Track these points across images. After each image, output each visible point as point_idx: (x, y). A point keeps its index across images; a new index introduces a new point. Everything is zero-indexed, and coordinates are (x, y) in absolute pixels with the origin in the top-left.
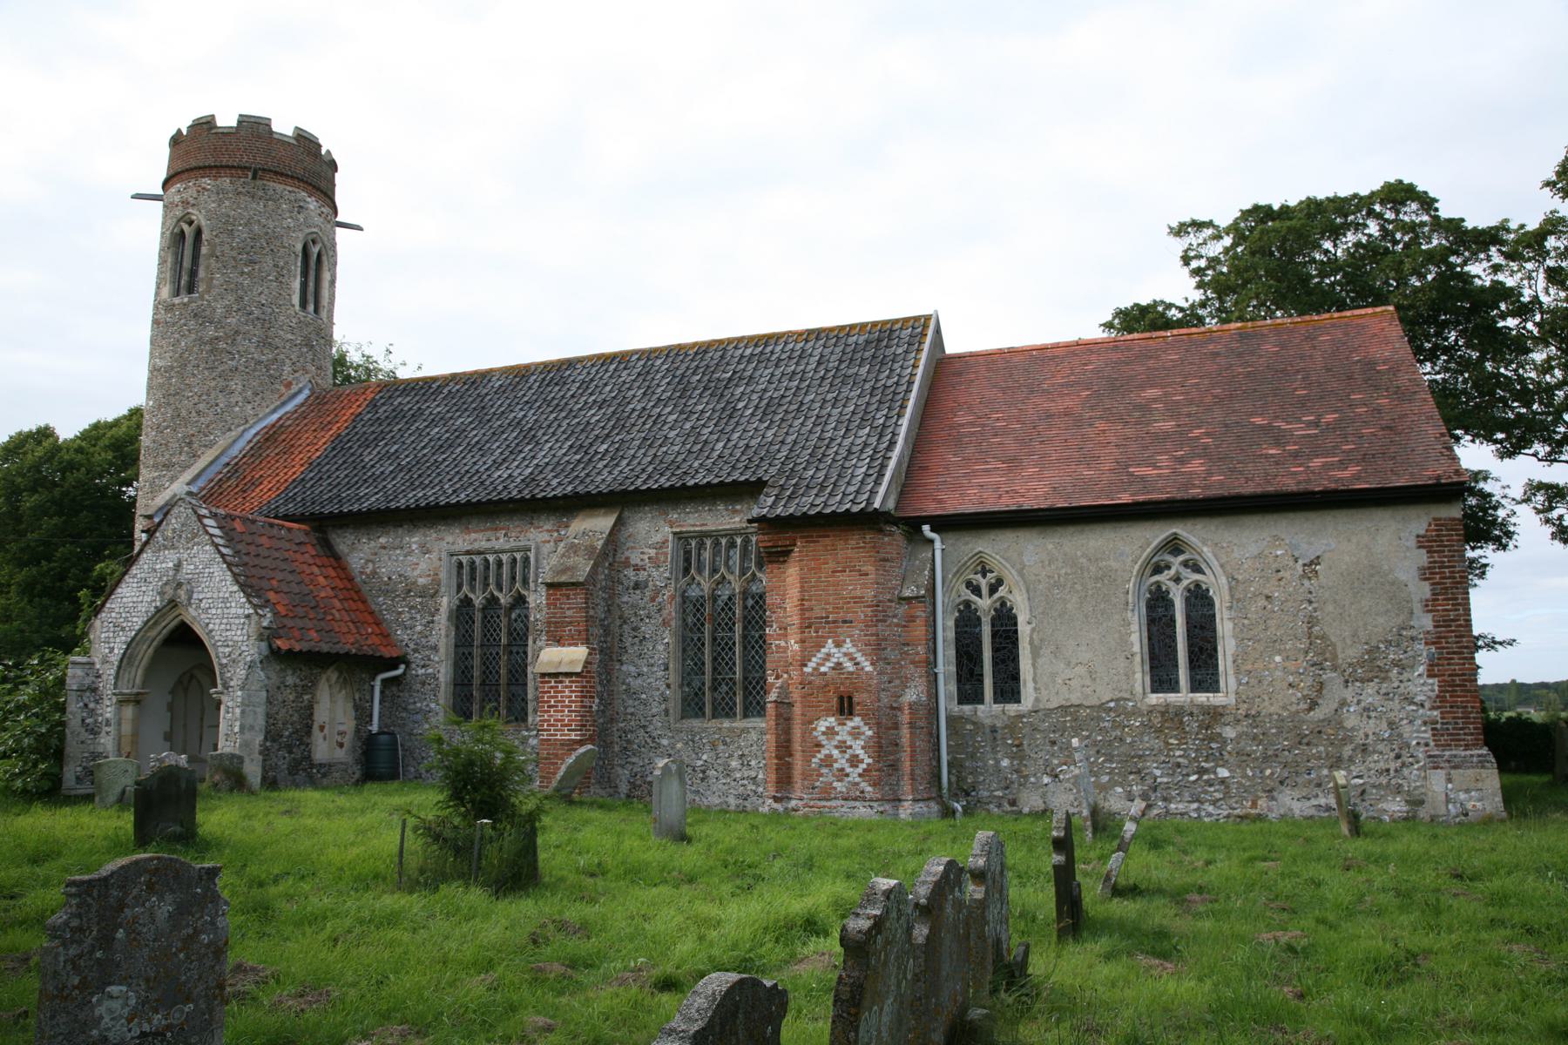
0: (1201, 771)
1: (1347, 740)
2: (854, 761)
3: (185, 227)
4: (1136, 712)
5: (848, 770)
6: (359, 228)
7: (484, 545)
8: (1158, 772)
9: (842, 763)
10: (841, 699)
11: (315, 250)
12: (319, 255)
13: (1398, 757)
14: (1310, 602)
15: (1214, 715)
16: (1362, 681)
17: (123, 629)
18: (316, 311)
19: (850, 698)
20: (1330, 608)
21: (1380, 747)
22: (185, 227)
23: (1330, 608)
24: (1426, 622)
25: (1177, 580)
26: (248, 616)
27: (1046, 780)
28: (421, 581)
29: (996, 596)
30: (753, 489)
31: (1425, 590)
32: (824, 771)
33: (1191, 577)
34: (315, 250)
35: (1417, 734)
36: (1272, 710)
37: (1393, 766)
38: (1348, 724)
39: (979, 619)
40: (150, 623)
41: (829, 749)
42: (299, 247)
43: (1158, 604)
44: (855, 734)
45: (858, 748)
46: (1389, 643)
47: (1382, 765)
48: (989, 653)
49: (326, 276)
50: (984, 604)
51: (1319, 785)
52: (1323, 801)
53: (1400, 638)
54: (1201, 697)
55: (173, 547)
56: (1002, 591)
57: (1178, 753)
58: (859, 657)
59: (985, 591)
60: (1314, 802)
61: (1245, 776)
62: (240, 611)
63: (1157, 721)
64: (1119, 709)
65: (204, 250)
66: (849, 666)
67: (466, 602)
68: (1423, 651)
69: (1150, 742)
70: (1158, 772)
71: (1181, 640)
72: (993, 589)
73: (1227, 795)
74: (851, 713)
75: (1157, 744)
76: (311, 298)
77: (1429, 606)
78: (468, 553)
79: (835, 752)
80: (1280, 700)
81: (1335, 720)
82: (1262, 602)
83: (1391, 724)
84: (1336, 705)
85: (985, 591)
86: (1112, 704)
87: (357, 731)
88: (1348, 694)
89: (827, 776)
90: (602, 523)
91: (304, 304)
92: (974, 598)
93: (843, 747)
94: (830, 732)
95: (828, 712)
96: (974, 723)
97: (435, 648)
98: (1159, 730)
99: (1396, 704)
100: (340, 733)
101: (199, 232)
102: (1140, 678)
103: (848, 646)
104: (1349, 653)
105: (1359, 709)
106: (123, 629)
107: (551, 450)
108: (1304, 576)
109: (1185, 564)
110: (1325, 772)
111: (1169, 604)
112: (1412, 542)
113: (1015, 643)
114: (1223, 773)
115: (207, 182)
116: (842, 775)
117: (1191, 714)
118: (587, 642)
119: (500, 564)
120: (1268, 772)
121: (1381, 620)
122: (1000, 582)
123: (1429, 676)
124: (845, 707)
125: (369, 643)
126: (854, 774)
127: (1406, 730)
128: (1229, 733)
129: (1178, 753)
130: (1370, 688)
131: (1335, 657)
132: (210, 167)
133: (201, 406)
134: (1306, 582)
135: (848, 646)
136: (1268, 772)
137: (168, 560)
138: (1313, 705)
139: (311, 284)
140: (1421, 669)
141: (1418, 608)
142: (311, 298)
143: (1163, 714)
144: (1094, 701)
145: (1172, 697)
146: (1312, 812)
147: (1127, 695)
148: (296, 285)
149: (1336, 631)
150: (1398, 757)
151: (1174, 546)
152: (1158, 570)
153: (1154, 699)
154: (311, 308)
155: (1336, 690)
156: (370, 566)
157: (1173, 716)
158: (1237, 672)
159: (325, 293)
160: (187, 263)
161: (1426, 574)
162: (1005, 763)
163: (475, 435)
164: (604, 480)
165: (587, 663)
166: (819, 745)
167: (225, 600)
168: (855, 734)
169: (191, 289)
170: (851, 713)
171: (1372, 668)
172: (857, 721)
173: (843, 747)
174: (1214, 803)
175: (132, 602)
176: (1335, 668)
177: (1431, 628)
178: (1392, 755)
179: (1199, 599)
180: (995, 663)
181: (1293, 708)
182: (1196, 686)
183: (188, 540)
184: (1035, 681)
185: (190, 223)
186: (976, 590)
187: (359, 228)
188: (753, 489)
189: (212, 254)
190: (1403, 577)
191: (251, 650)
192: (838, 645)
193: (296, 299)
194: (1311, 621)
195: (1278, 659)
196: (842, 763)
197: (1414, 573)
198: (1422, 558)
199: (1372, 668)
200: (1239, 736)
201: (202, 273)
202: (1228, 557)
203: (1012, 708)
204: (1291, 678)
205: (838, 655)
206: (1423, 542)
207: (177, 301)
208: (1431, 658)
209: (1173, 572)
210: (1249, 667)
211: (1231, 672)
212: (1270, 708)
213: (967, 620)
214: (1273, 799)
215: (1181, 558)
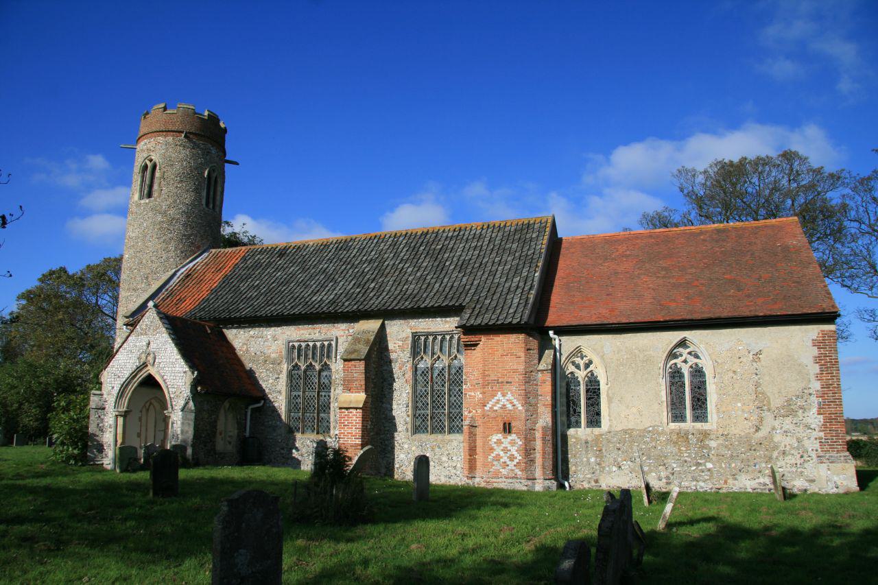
0: (698, 464)
1: (775, 447)
2: (512, 458)
3: (148, 163)
4: (663, 433)
5: (509, 463)
6: (237, 164)
7: (307, 337)
8: (675, 465)
9: (505, 459)
10: (505, 424)
12: (216, 178)
13: (802, 457)
14: (757, 374)
15: (706, 435)
16: (784, 417)
17: (119, 377)
19: (510, 424)
21: (792, 452)
22: (148, 163)
24: (816, 386)
25: (685, 361)
26: (185, 372)
27: (614, 469)
28: (273, 356)
29: (589, 370)
32: (495, 463)
35: (812, 445)
36: (736, 432)
37: (799, 462)
38: (776, 440)
39: (579, 382)
40: (134, 375)
41: (498, 451)
43: (675, 376)
44: (513, 443)
45: (514, 451)
46: (798, 397)
47: (793, 461)
49: (219, 189)
51: (760, 472)
52: (761, 480)
53: (804, 394)
54: (698, 425)
55: (146, 334)
56: (592, 367)
57: (685, 455)
58: (516, 402)
59: (582, 367)
60: (757, 481)
61: (721, 467)
62: (181, 369)
63: (674, 437)
64: (654, 433)
65: (158, 174)
66: (509, 406)
67: (296, 367)
68: (815, 400)
69: (670, 449)
70: (675, 465)
71: (688, 395)
72: (587, 366)
73: (711, 476)
74: (509, 432)
75: (675, 450)
76: (211, 201)
77: (819, 377)
78: (299, 341)
79: (502, 453)
80: (740, 428)
81: (769, 437)
82: (731, 374)
83: (799, 441)
84: (769, 430)
85: (582, 367)
86: (651, 429)
87: (238, 436)
88: (776, 423)
89: (497, 466)
90: (373, 325)
91: (207, 204)
92: (576, 370)
93: (505, 450)
94: (499, 442)
96: (576, 438)
97: (280, 392)
98: (675, 443)
99: (801, 429)
100: (230, 437)
101: (154, 167)
102: (664, 414)
103: (509, 396)
104: (777, 402)
105: (782, 432)
106: (119, 377)
107: (344, 286)
108: (754, 361)
109: (690, 353)
110: (764, 465)
111: (681, 376)
112: (810, 343)
113: (598, 395)
114: (709, 465)
115: (161, 139)
116: (505, 465)
117: (693, 434)
119: (315, 346)
120: (733, 465)
121: (793, 384)
122: (591, 362)
123: (818, 414)
124: (507, 428)
126: (511, 465)
127: (806, 443)
128: (713, 444)
129: (685, 455)
130: (788, 420)
131: (769, 403)
132: (162, 131)
133: (153, 258)
134: (754, 364)
135: (509, 396)
136: (733, 465)
137: (143, 341)
138: (758, 429)
139: (212, 193)
140: (815, 410)
141: (813, 378)
142: (211, 201)
143: (678, 434)
144: (641, 427)
145: (682, 425)
146: (757, 486)
147: (657, 423)
149: (769, 389)
150: (802, 457)
152: (676, 356)
153: (673, 426)
154: (211, 206)
156: (245, 347)
157: (684, 436)
158: (718, 411)
159: (218, 198)
160: (148, 182)
161: (818, 360)
162: (593, 460)
163: (301, 277)
164: (375, 303)
165: (365, 402)
166: (492, 449)
167: (173, 363)
168: (513, 443)
169: (150, 195)
170: (509, 432)
171: (789, 410)
172: (513, 436)
173: (505, 450)
174: (704, 481)
176: (769, 410)
177: (819, 389)
178: (799, 456)
179: (698, 373)
180: (588, 406)
181: (747, 431)
182: (697, 418)
183: (154, 330)
184: (609, 416)
185: (151, 160)
186: (578, 367)
187: (237, 164)
189: (163, 177)
191: (187, 392)
192: (504, 395)
194: (757, 385)
195: (739, 405)
196: (505, 459)
197: (811, 360)
198: (815, 351)
199: (789, 410)
200: (718, 445)
201: (156, 187)
203: (596, 431)
204: (746, 415)
205: (503, 401)
206: (816, 343)
207: (142, 202)
208: (819, 404)
209: (683, 358)
210: (724, 409)
211: (714, 411)
214: (736, 479)
215: (688, 350)
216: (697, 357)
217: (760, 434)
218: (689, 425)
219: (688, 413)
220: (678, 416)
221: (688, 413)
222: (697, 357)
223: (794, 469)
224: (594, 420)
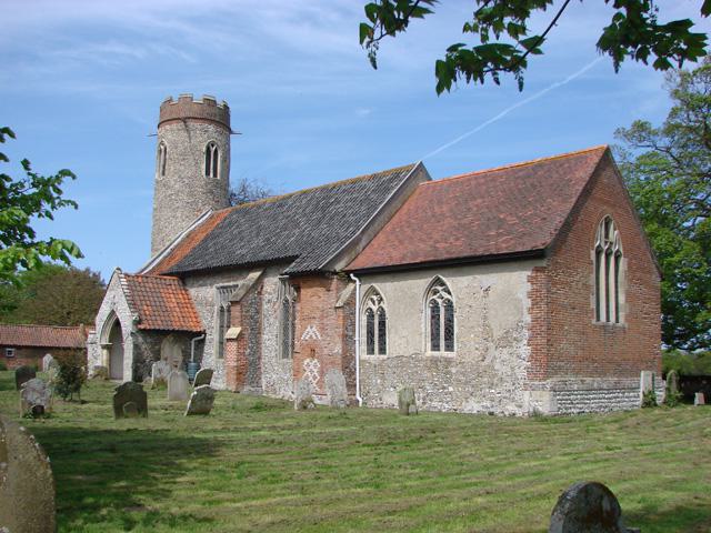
0: (444, 388)
11: (213, 149)
12: (216, 151)
15: (448, 361)
18: (215, 175)
20: (493, 312)
23: (493, 312)
24: (528, 319)
30: (289, 260)
31: (528, 303)
33: (446, 296)
34: (213, 149)
35: (521, 373)
42: (204, 149)
43: (435, 308)
44: (315, 366)
45: (316, 370)
48: (378, 333)
50: (375, 308)
53: (518, 328)
54: (436, 353)
63: (429, 363)
64: (415, 358)
68: (527, 333)
69: (427, 374)
71: (442, 332)
75: (429, 375)
76: (212, 171)
77: (530, 310)
80: (472, 356)
88: (497, 353)
91: (208, 173)
94: (308, 365)
95: (308, 357)
104: (498, 333)
114: (451, 389)
115: (168, 127)
118: (242, 325)
121: (511, 318)
125: (190, 326)
127: (517, 371)
140: (525, 342)
141: (525, 311)
142: (212, 171)
148: (204, 166)
149: (494, 324)
151: (439, 282)
153: (429, 353)
155: (493, 352)
157: (435, 361)
160: (162, 163)
161: (530, 295)
168: (308, 365)
169: (164, 174)
172: (316, 360)
173: (311, 371)
175: (104, 310)
179: (449, 306)
188: (289, 260)
190: (521, 296)
193: (204, 173)
199: (506, 341)
202: (460, 286)
203: (385, 357)
212: (467, 359)
213: (371, 316)
216: (450, 293)
217: (486, 362)
218: (443, 353)
219: (442, 343)
220: (436, 347)
221: (442, 343)
222: (450, 293)
223: (508, 395)
224: (382, 350)
